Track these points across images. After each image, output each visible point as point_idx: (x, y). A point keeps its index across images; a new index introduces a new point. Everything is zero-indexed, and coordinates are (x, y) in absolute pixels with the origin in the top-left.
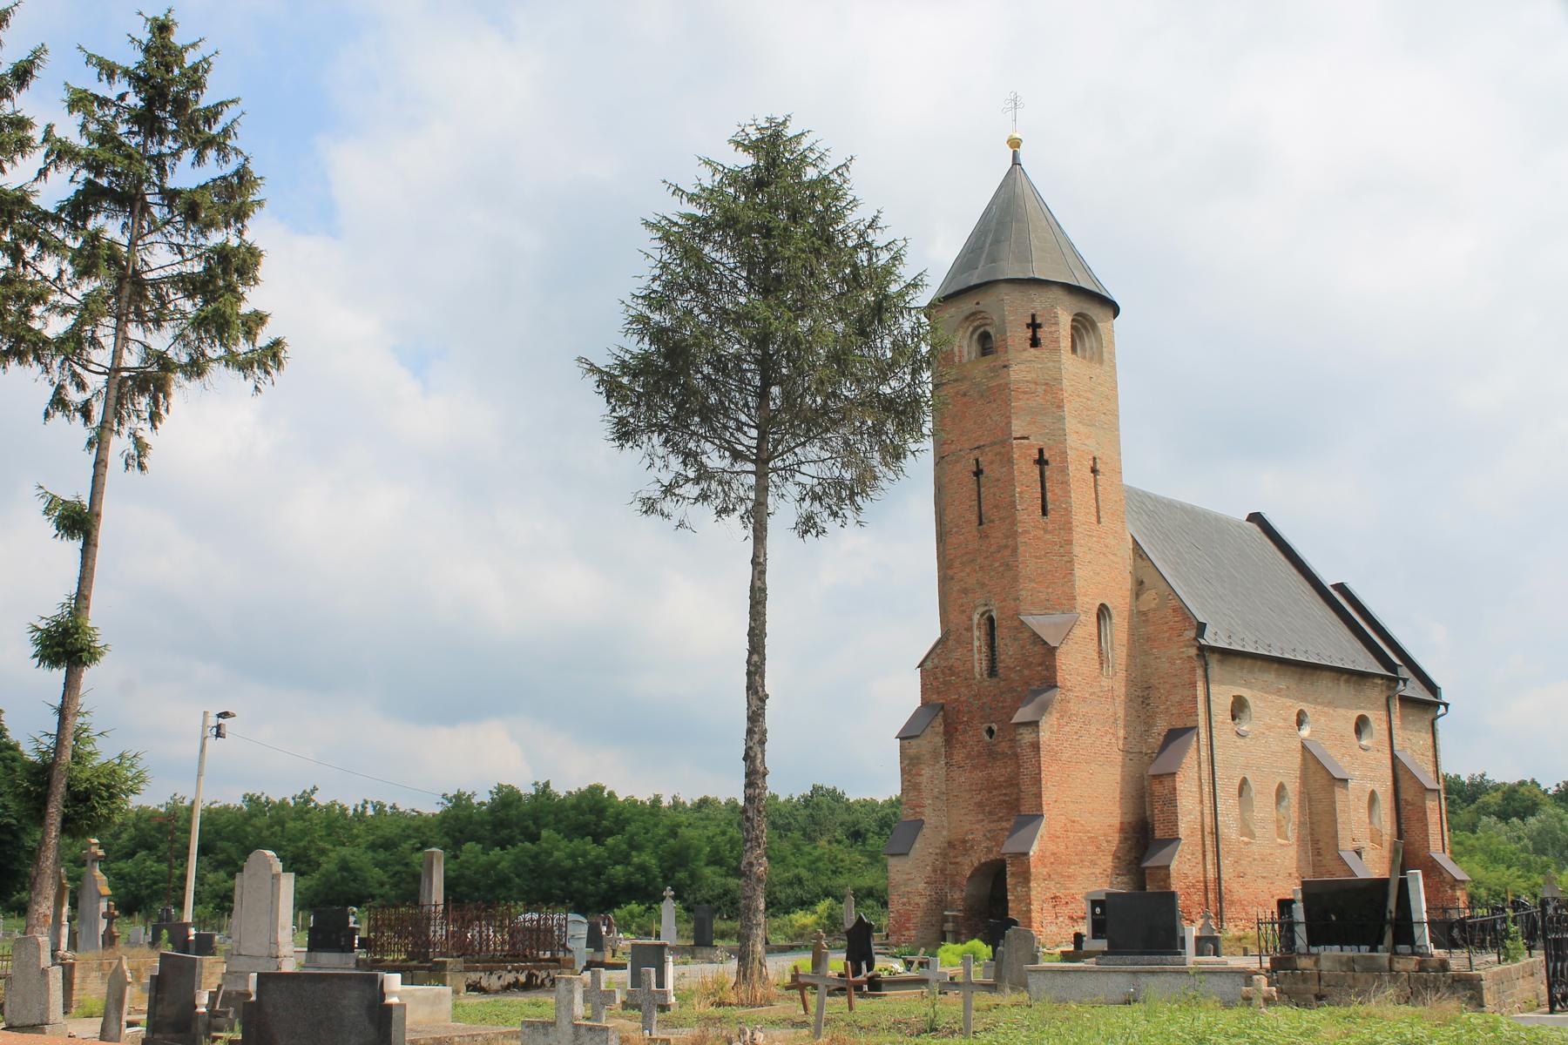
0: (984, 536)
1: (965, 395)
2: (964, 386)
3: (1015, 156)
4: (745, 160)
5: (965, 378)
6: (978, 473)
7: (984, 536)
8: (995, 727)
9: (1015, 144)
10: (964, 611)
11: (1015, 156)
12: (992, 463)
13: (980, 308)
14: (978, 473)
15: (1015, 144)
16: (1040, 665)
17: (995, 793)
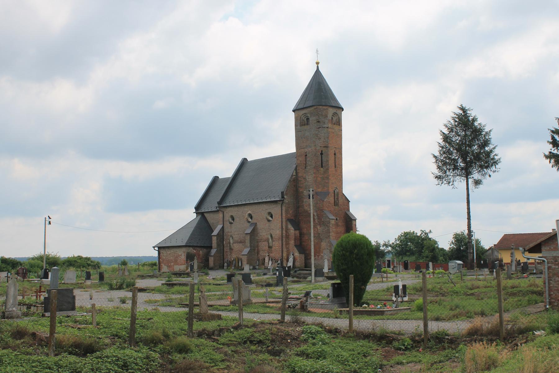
0: (336, 171)
1: (333, 133)
2: (333, 131)
3: (318, 67)
4: (461, 112)
5: (333, 129)
6: (335, 154)
7: (336, 171)
8: (338, 218)
9: (318, 63)
10: (332, 188)
11: (318, 67)
12: (338, 153)
13: (337, 112)
14: (335, 154)
15: (318, 63)
16: (347, 205)
17: (338, 234)
